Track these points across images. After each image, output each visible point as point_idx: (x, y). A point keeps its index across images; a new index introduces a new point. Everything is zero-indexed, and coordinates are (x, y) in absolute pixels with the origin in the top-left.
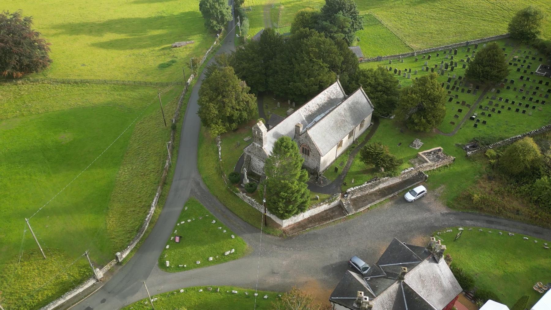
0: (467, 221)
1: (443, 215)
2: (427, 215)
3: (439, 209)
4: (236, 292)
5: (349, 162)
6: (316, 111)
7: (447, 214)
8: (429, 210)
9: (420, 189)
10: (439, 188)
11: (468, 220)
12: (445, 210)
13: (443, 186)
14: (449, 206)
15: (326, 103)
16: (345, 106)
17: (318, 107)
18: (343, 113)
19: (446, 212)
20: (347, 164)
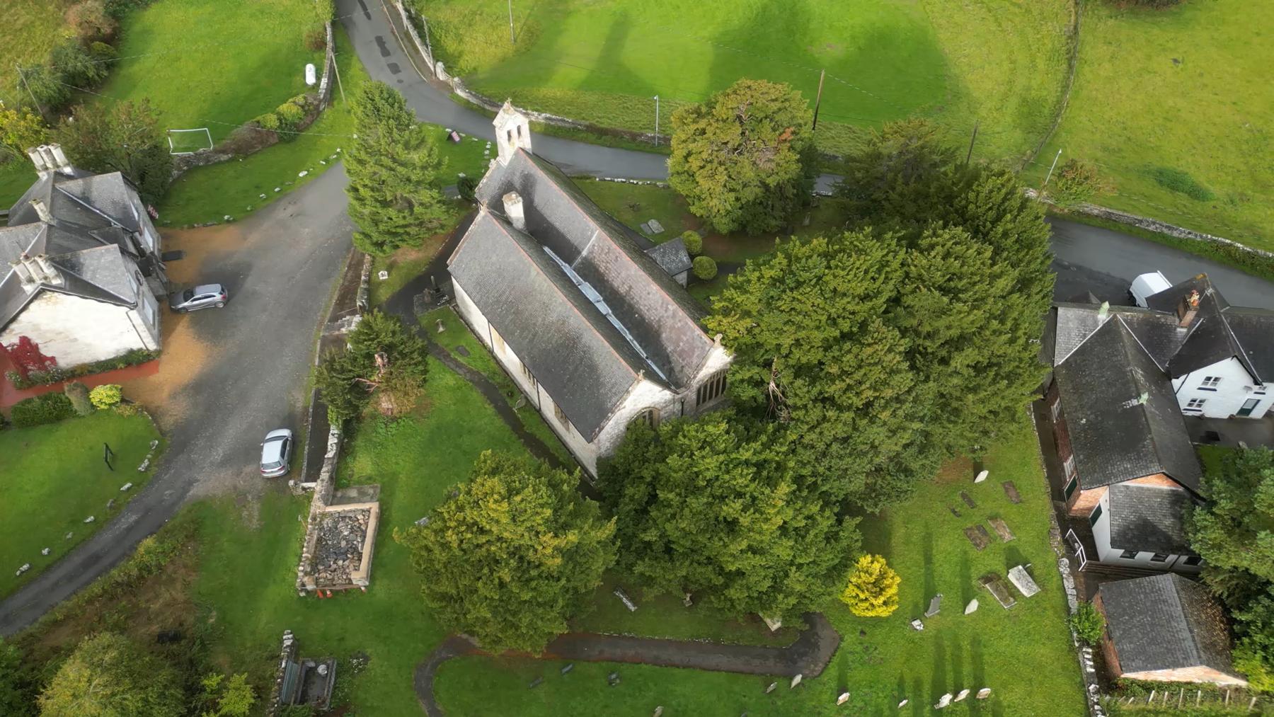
0: (134, 518)
1: (190, 483)
2: (218, 454)
3: (209, 481)
4: (301, 175)
5: (459, 365)
6: (612, 288)
7: (186, 491)
8: (226, 462)
9: (272, 453)
10: (256, 513)
11: (137, 522)
12: (197, 491)
13: (255, 524)
14: (202, 503)
15: (642, 319)
16: (572, 321)
17: (622, 290)
18: (553, 317)
19: (191, 493)
20: (455, 360)
